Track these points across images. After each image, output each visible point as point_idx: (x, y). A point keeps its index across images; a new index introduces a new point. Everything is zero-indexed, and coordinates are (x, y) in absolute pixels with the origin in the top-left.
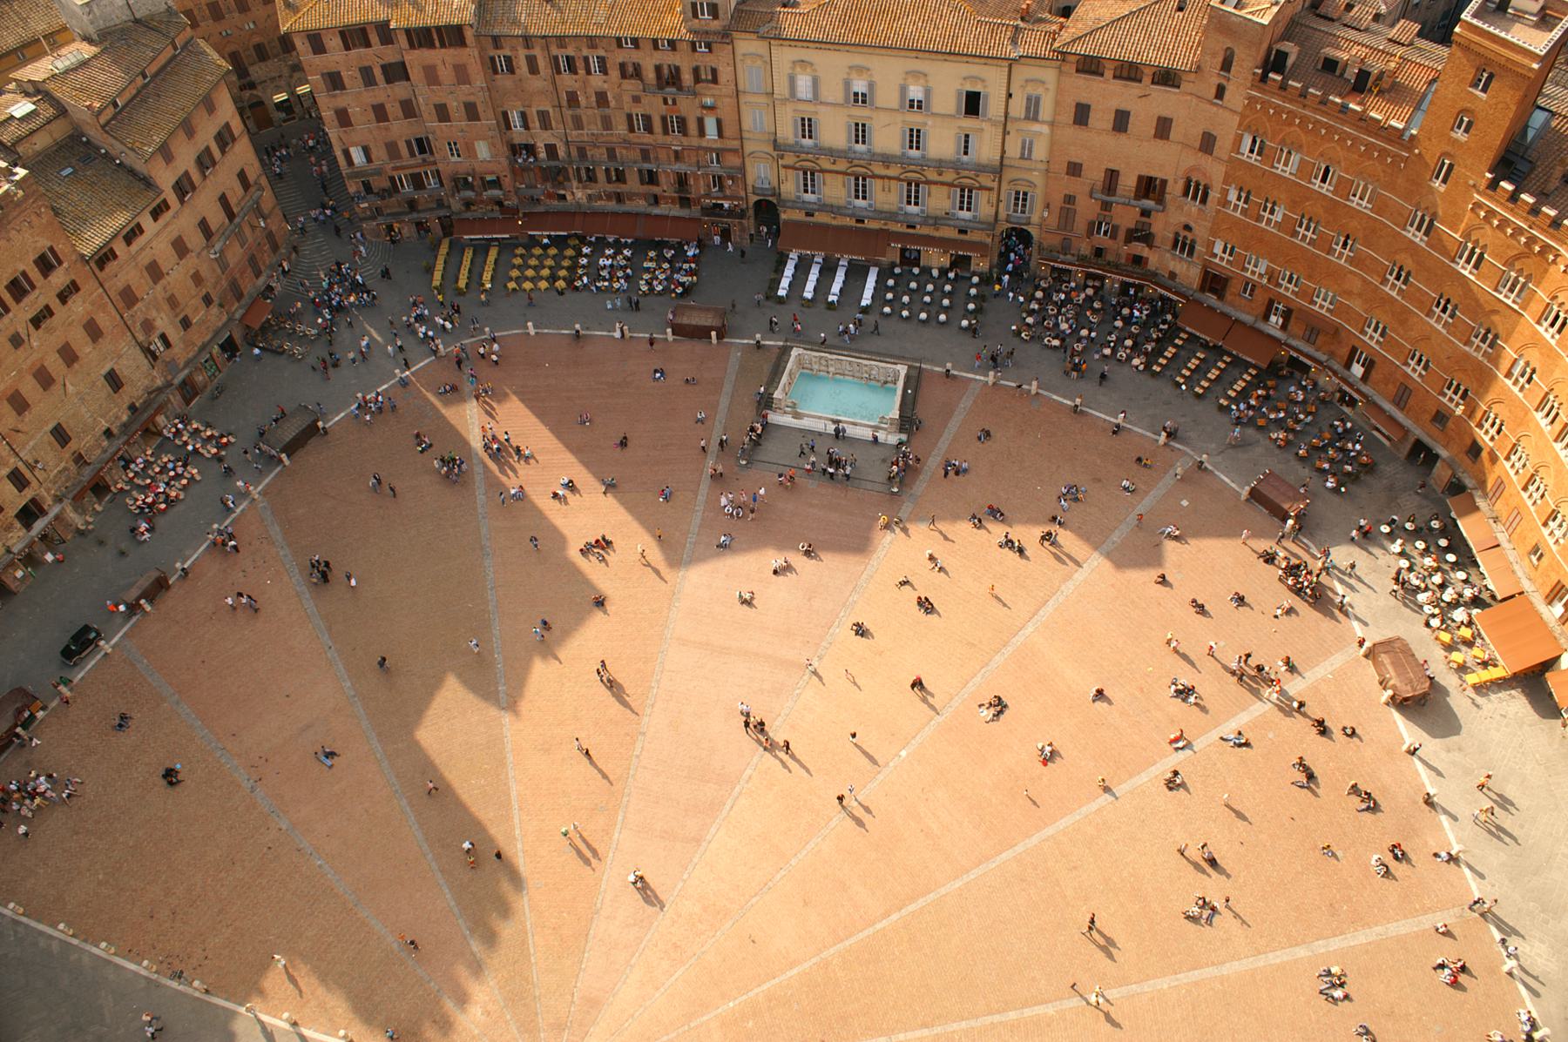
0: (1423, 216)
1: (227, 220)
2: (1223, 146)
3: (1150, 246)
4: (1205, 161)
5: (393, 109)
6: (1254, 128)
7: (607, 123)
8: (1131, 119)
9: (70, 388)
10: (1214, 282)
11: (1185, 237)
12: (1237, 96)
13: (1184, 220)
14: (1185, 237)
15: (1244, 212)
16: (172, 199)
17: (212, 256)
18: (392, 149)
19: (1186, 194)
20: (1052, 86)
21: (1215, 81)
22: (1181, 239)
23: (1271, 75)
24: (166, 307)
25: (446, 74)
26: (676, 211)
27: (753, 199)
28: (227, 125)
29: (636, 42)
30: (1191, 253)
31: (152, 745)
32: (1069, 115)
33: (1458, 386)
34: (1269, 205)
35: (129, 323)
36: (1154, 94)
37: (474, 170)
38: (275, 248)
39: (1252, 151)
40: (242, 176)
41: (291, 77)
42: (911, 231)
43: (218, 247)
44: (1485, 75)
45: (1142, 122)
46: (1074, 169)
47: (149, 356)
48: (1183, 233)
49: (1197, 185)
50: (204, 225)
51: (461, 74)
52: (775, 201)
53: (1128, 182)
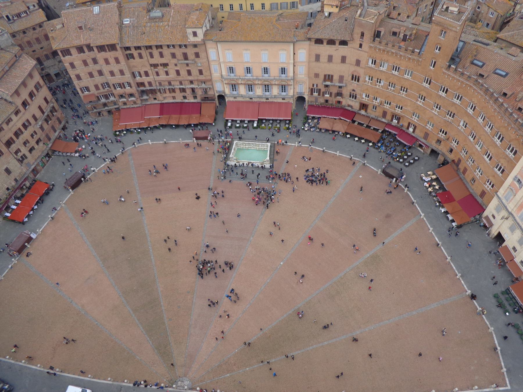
0: (428, 79)
1: (42, 114)
2: (362, 64)
3: (342, 98)
4: (358, 69)
5: (96, 74)
6: (372, 56)
7: (167, 73)
8: (333, 58)
10: (364, 106)
11: (353, 94)
12: (365, 46)
13: (352, 88)
14: (353, 94)
15: (371, 83)
16: (21, 108)
17: (38, 127)
18: (97, 87)
19: (352, 79)
21: (359, 43)
22: (352, 94)
23: (377, 39)
25: (112, 61)
27: (217, 95)
28: (38, 83)
29: (173, 46)
30: (356, 98)
32: (313, 59)
33: (443, 131)
34: (379, 81)
36: (340, 49)
37: (125, 92)
38: (60, 122)
39: (372, 64)
40: (45, 99)
41: (59, 65)
42: (268, 100)
43: (40, 123)
44: (443, 32)
45: (337, 58)
46: (317, 75)
47: (19, 162)
48: (352, 92)
49: (356, 77)
50: (34, 117)
51: (117, 61)
52: (224, 95)
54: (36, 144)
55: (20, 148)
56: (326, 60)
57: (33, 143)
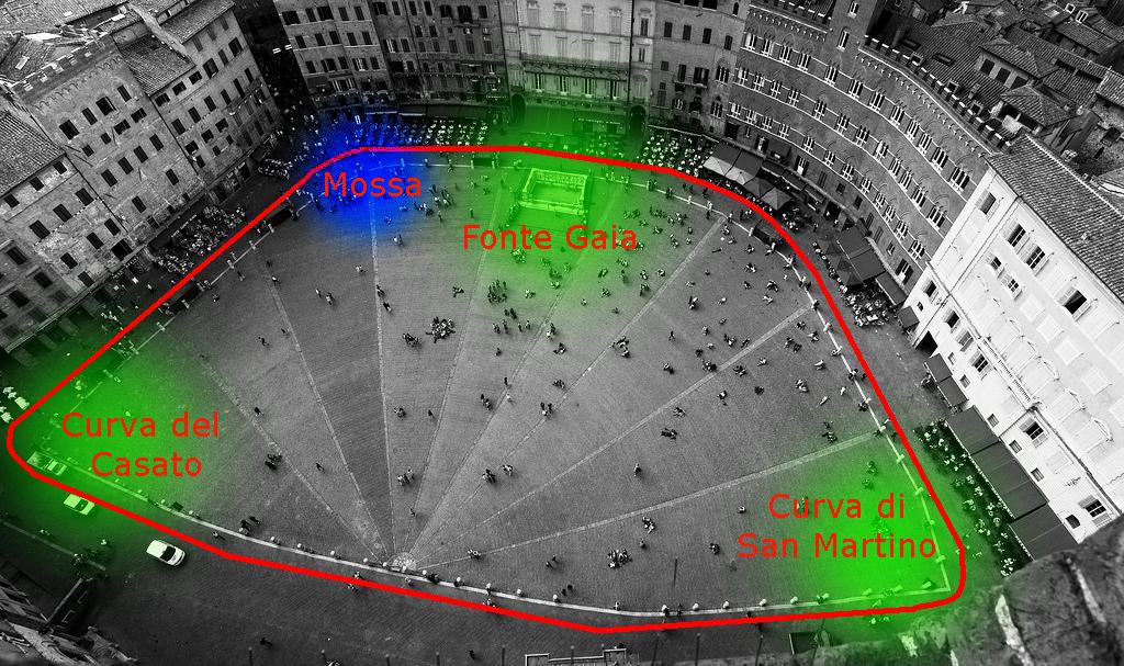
9: (144, 176)
20: (653, 13)
26: (475, 103)
46: (665, 66)
53: (690, 72)
55: (196, 141)
56: (680, 36)
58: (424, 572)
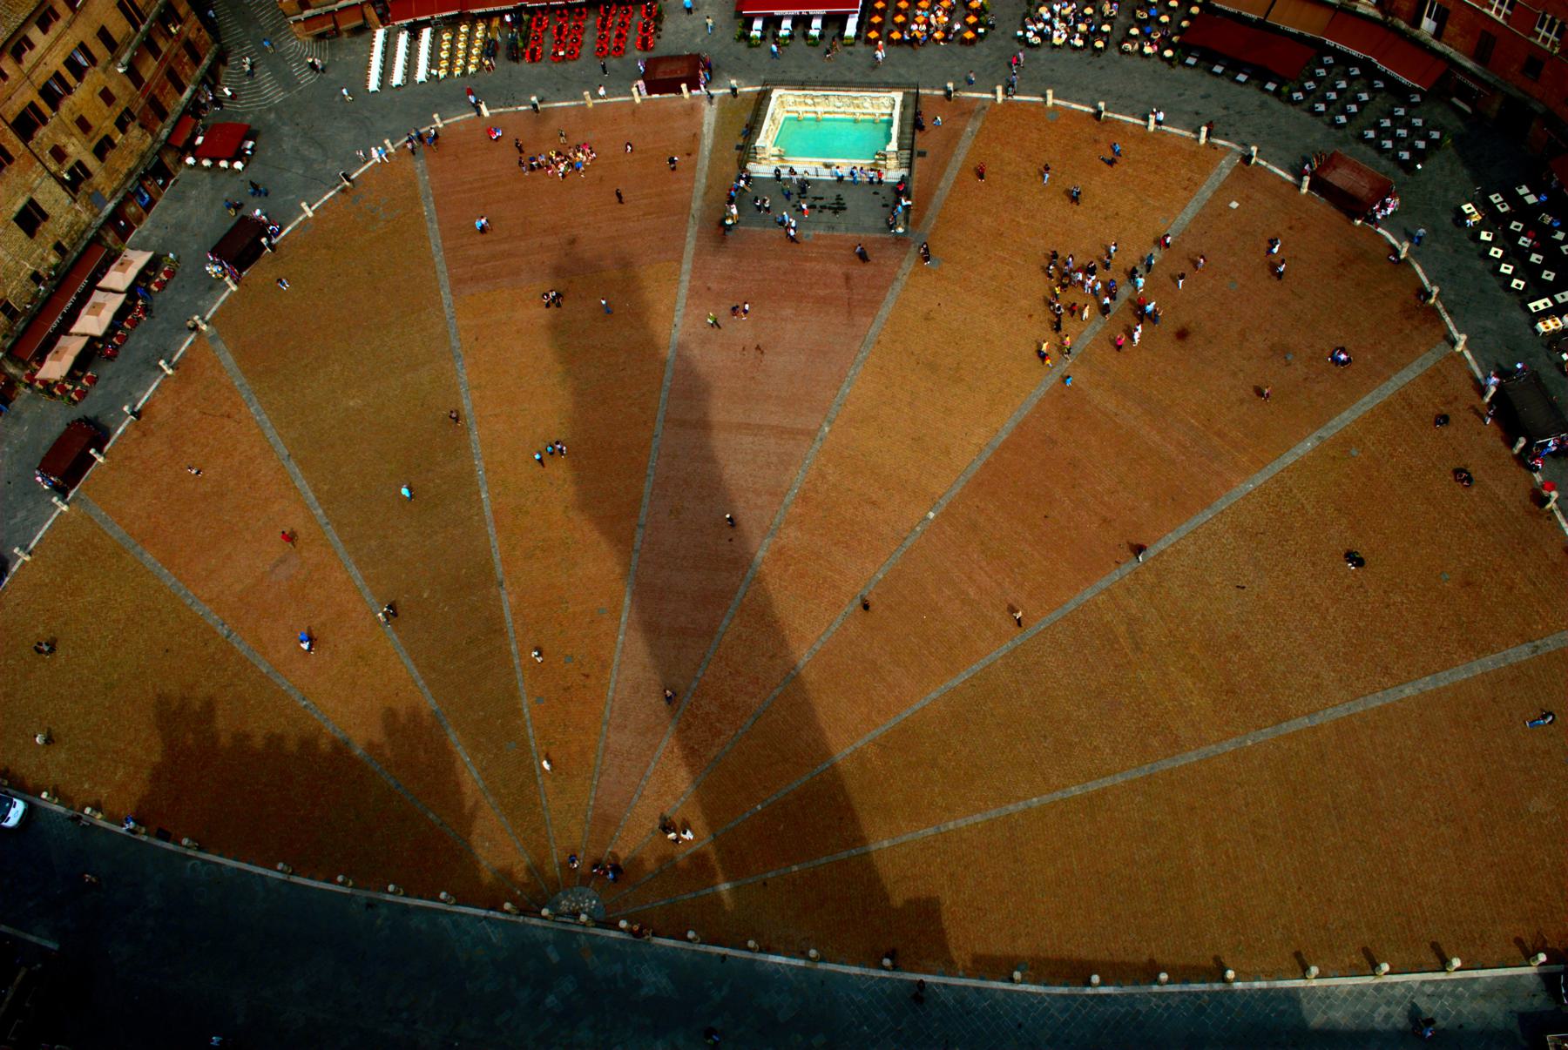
1: (132, 29)
24: (76, 130)
31: (120, 600)
35: (36, 151)
43: (125, 58)
47: (67, 188)
50: (104, 35)
54: (116, 129)
57: (104, 122)
58: (623, 924)
